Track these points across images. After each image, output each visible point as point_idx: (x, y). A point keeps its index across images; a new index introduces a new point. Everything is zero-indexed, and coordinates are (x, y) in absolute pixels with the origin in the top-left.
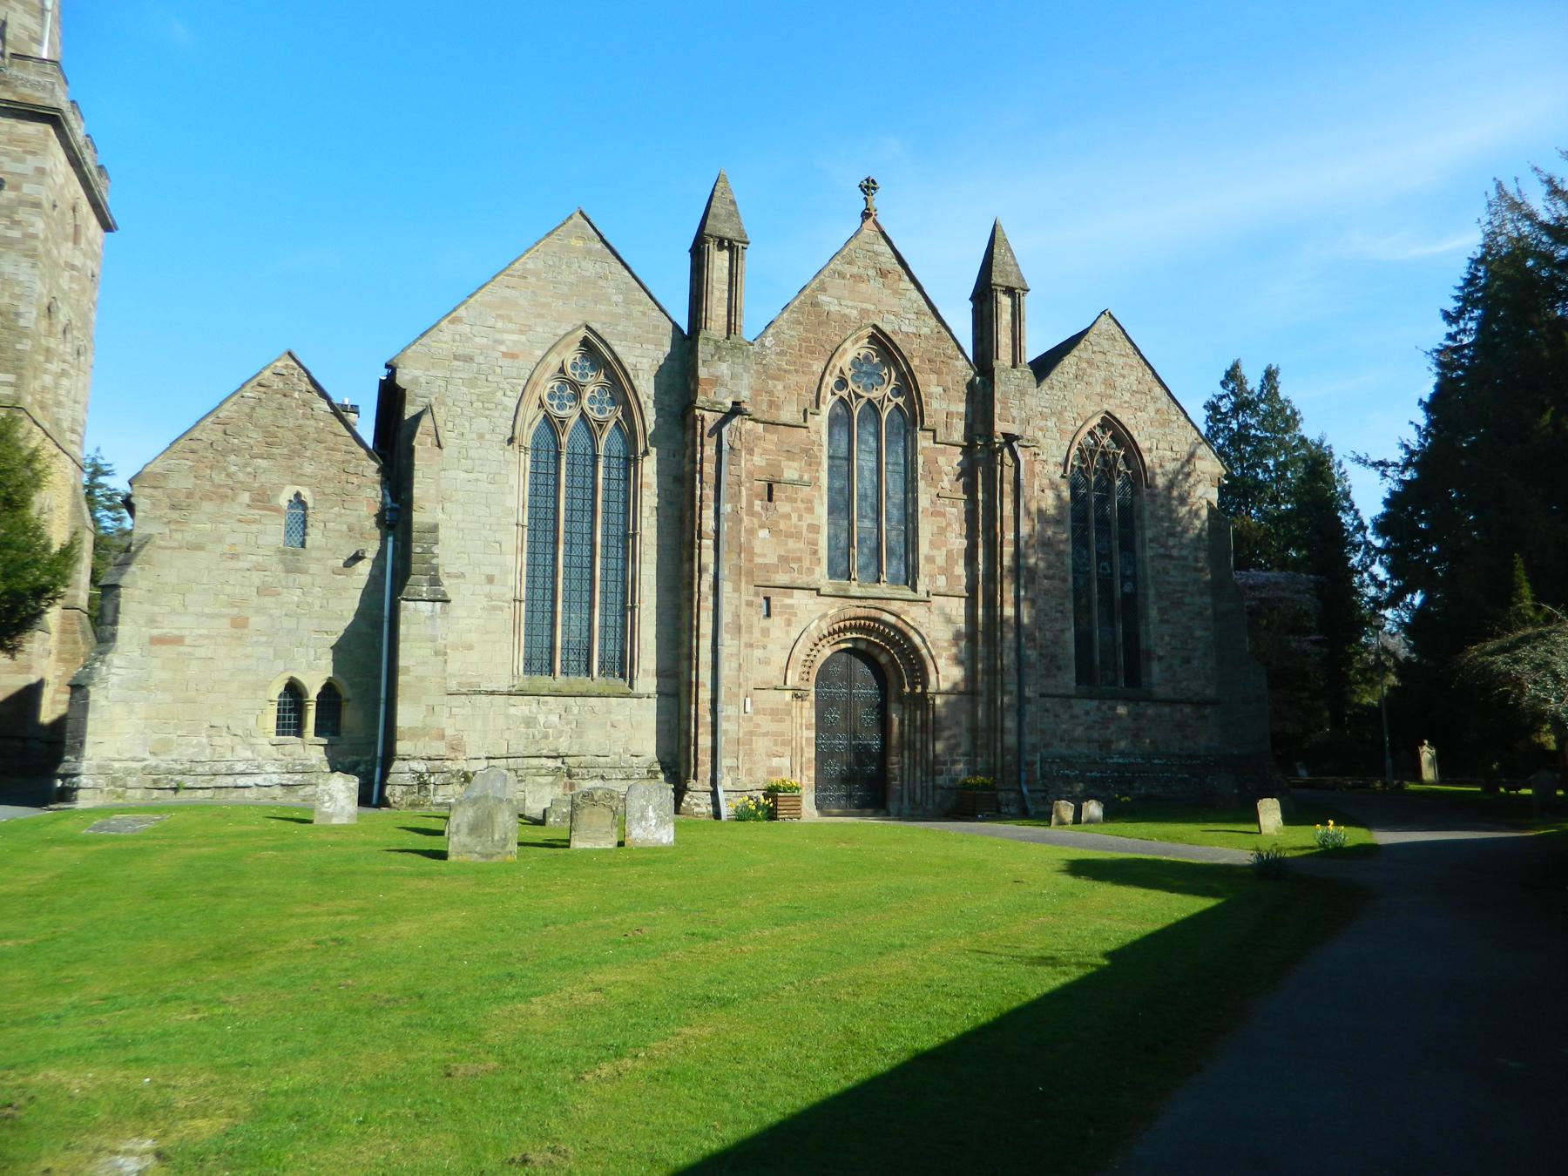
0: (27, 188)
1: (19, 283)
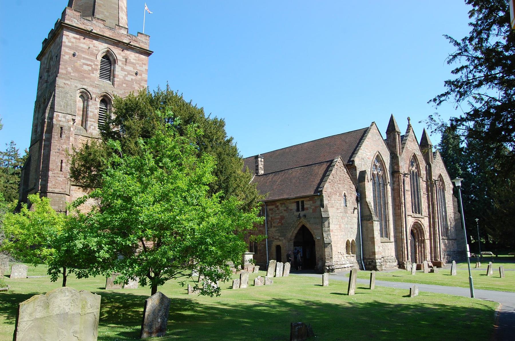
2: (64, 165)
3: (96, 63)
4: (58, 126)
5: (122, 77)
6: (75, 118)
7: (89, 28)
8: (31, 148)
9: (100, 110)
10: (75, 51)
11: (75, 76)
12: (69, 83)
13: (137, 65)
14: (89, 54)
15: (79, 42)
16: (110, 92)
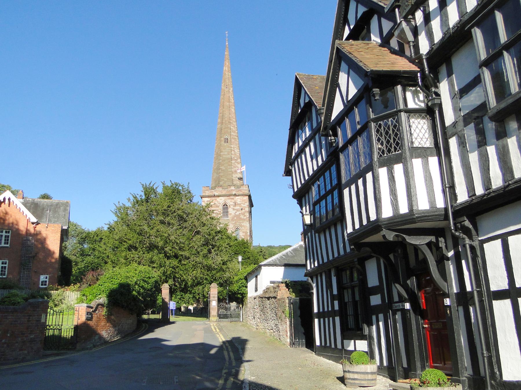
1: (247, 227)
3: (219, 211)
5: (234, 214)
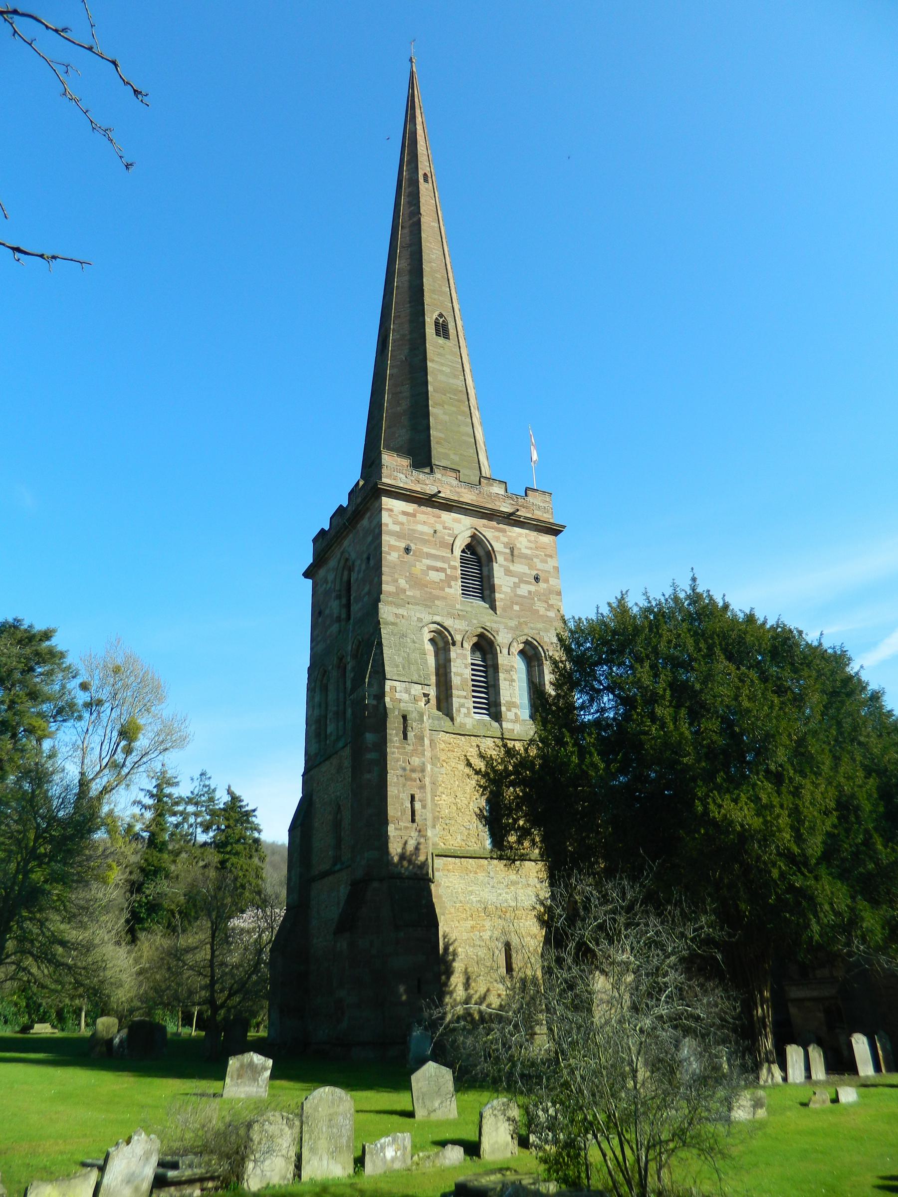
0: (552, 581)
2: (418, 806)
3: (452, 563)
4: (397, 713)
5: (509, 590)
6: (429, 691)
7: (431, 489)
8: (312, 773)
9: (472, 670)
10: (408, 542)
11: (413, 597)
12: (405, 614)
13: (535, 560)
14: (436, 544)
15: (413, 522)
16: (488, 625)
